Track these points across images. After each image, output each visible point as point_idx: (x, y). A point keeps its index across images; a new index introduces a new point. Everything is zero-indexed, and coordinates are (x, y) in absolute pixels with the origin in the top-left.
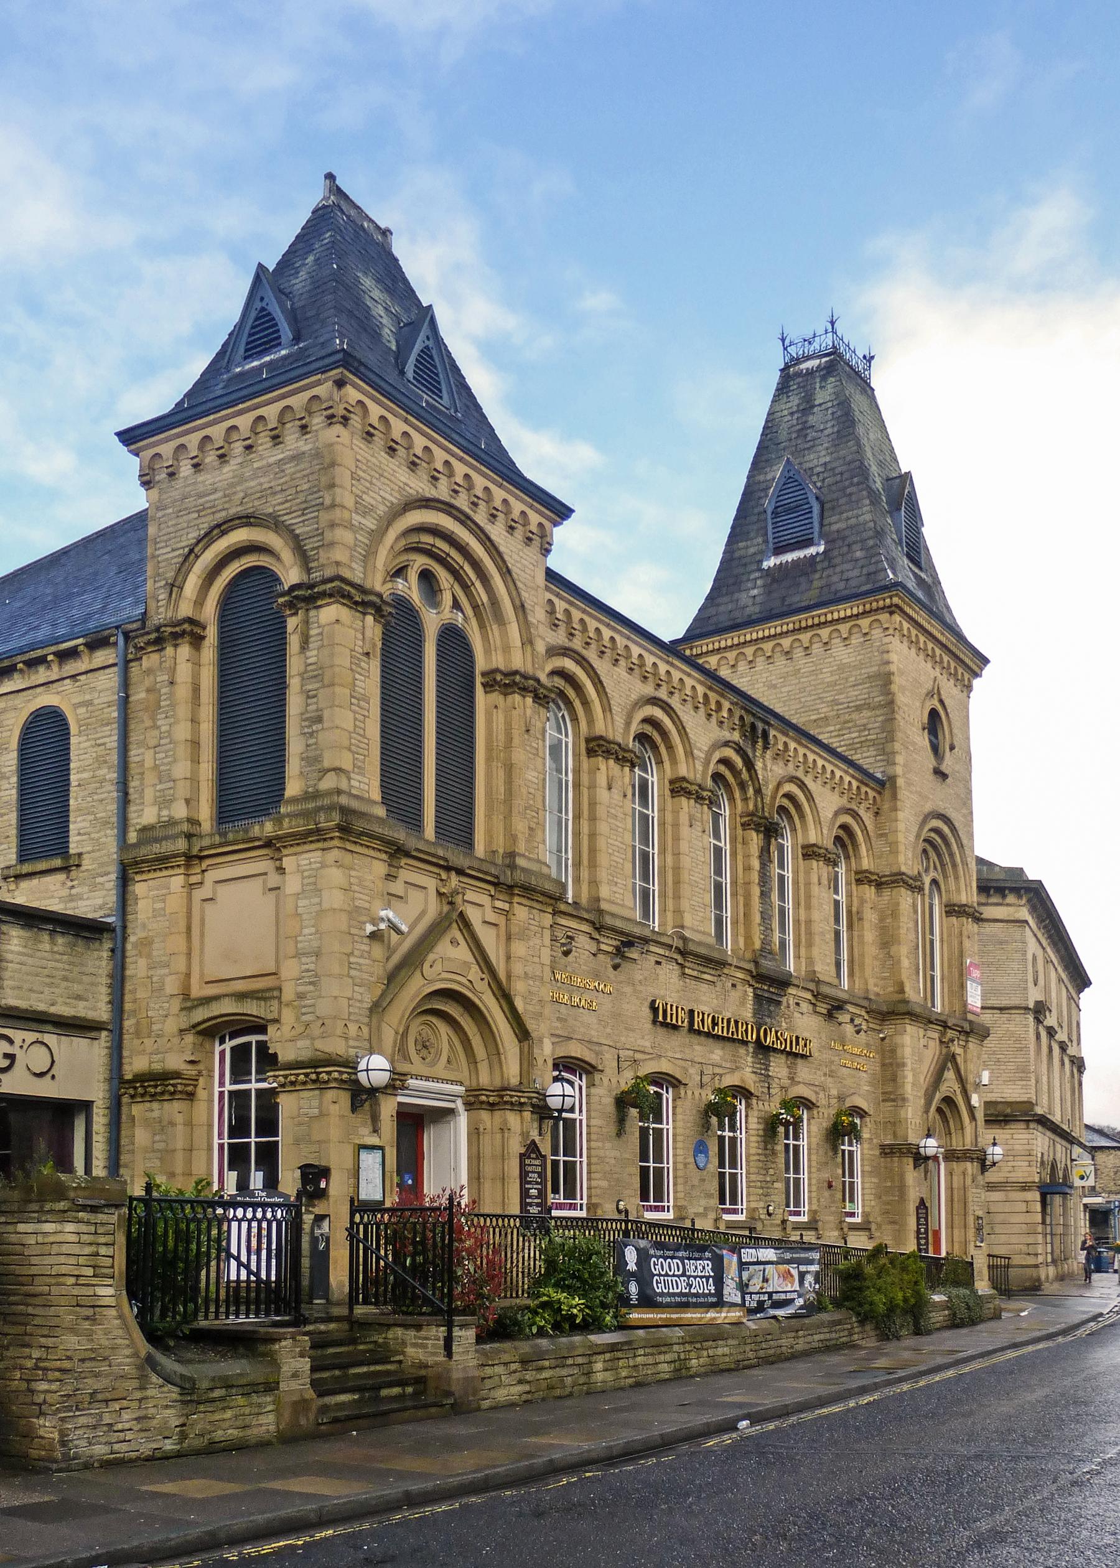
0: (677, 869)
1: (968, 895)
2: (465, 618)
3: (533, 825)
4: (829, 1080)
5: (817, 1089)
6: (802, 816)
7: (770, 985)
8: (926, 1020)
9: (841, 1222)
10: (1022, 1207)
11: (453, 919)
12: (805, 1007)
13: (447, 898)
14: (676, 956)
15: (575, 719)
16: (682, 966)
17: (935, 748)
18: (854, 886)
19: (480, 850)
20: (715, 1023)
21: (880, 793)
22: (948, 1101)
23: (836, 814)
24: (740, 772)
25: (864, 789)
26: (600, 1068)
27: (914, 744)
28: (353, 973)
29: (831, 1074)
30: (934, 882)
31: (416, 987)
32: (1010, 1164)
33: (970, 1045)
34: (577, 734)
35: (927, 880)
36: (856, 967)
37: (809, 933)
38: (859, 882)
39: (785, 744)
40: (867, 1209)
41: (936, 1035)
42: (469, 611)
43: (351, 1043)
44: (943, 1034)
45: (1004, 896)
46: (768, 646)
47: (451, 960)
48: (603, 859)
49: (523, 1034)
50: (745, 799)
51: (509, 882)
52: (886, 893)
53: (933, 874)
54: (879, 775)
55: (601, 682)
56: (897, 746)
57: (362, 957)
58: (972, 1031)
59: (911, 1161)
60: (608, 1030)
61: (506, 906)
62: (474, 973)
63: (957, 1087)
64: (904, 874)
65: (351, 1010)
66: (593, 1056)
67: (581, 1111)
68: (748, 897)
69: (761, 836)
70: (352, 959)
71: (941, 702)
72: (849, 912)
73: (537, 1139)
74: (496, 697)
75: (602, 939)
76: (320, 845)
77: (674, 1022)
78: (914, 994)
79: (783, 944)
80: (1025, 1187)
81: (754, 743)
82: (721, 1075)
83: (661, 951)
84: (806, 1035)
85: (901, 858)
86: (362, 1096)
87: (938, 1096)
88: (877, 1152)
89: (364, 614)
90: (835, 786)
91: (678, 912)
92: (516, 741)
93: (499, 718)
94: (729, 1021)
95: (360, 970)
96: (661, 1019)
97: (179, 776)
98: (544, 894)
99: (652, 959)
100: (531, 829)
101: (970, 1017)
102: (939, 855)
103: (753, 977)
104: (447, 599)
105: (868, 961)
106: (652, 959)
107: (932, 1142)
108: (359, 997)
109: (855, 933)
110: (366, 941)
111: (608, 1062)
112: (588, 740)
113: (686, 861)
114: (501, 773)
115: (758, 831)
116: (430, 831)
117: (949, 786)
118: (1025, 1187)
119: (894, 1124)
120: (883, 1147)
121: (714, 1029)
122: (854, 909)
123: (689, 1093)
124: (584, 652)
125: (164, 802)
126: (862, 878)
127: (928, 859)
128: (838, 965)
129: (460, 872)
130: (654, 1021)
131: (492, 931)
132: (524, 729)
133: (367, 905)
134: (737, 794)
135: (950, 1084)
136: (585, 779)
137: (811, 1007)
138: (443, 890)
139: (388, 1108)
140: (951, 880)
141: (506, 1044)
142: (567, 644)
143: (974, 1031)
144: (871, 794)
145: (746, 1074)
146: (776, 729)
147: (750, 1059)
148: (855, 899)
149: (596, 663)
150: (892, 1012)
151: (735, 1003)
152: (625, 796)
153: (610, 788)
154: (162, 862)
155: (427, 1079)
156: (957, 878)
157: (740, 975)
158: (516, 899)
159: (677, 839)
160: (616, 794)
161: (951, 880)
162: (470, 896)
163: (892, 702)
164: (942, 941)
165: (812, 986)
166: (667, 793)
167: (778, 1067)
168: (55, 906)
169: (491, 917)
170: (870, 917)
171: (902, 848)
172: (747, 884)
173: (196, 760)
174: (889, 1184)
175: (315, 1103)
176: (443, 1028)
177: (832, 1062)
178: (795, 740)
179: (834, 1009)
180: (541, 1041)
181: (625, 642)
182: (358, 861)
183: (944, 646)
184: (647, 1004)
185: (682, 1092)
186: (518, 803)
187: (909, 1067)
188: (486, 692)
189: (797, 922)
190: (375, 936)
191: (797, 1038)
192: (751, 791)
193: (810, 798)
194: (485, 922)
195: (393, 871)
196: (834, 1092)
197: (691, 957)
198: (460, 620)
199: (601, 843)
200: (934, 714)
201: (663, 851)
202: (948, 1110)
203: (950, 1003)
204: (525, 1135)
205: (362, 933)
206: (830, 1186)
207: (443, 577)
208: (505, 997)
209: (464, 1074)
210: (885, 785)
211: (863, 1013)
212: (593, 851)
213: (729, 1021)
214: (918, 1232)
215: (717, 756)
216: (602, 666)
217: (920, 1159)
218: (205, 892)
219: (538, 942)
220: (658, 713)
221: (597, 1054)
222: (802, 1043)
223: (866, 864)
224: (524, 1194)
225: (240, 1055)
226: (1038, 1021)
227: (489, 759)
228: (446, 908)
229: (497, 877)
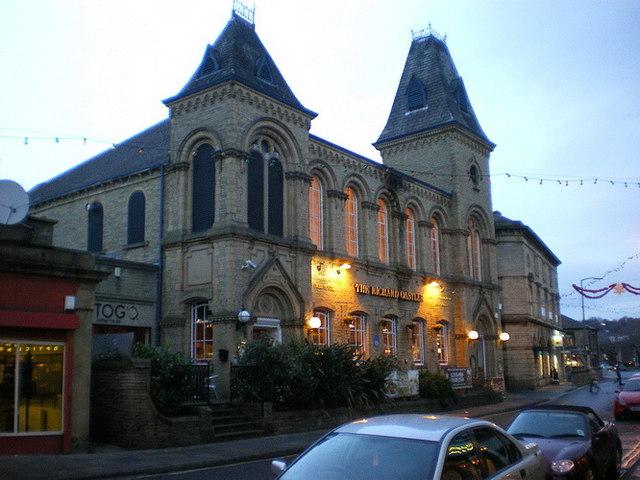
1: (491, 235)
6: (418, 211)
10: (525, 356)
11: (274, 261)
13: (272, 254)
15: (323, 184)
17: (475, 181)
19: (285, 235)
20: (381, 291)
22: (483, 316)
23: (432, 208)
30: (476, 230)
31: (260, 287)
35: (473, 230)
42: (280, 151)
47: (273, 277)
48: (334, 234)
56: (458, 181)
62: (282, 280)
80: (527, 348)
86: (240, 325)
90: (429, 197)
97: (179, 215)
116: (266, 230)
118: (527, 348)
125: (175, 224)
128: (435, 266)
131: (289, 265)
135: (484, 309)
139: (250, 329)
143: (493, 288)
149: (330, 164)
154: (174, 245)
162: (280, 252)
168: (140, 260)
170: (448, 247)
173: (186, 209)
176: (272, 300)
183: (476, 142)
190: (244, 270)
193: (420, 204)
200: (473, 168)
207: (271, 142)
208: (294, 288)
210: (452, 197)
212: (330, 232)
215: (381, 191)
218: (188, 255)
220: (356, 179)
223: (446, 226)
225: (200, 311)
226: (530, 281)
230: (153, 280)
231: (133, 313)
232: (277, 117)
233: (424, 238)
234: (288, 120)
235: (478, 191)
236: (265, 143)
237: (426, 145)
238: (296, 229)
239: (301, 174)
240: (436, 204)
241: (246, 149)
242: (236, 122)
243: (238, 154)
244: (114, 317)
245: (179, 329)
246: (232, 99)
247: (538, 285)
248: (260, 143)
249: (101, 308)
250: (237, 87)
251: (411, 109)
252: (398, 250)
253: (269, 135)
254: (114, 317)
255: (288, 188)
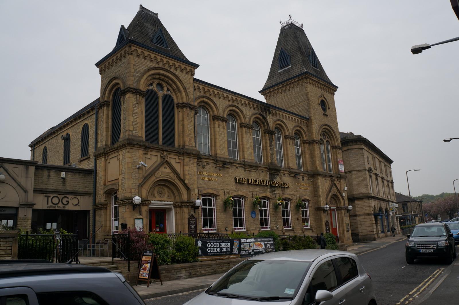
0: (243, 145)
2: (171, 92)
3: (190, 138)
4: (296, 193)
5: (292, 195)
7: (274, 170)
8: (325, 176)
9: (302, 228)
12: (286, 175)
14: (242, 166)
16: (245, 168)
18: (302, 145)
21: (307, 121)
22: (334, 195)
23: (294, 127)
24: (262, 120)
25: (302, 121)
26: (218, 195)
27: (316, 108)
28: (133, 177)
29: (297, 191)
30: (327, 141)
31: (153, 179)
32: (365, 209)
33: (341, 180)
34: (210, 116)
35: (325, 141)
36: (304, 164)
37: (288, 157)
38: (304, 143)
39: (276, 112)
40: (293, 225)
41: (330, 179)
43: (133, 194)
44: (332, 179)
45: (357, 143)
46: (280, 90)
47: (165, 172)
48: (218, 144)
49: (188, 188)
50: (264, 126)
51: (182, 152)
52: (311, 145)
53: (327, 139)
54: (307, 117)
55: (215, 103)
56: (311, 110)
57: (136, 173)
58: (341, 177)
59: (323, 212)
60: (221, 186)
61: (183, 158)
62: (172, 175)
63: (337, 191)
64: (315, 140)
65: (133, 186)
66: (216, 192)
67: (214, 206)
68: (267, 149)
69: (269, 134)
70: (133, 174)
71: (324, 98)
72: (302, 151)
73: (194, 214)
74: (180, 110)
75: (218, 164)
76: (125, 148)
77: (242, 182)
78: (320, 169)
79: (281, 160)
81: (266, 113)
82: (259, 194)
83: (238, 165)
84: (287, 182)
85: (314, 136)
87: (330, 194)
88: (314, 210)
89: (137, 95)
91: (243, 155)
92: (185, 118)
93: (181, 114)
94: (260, 181)
95: (136, 176)
96: (237, 182)
98: (193, 154)
99: (235, 167)
100: (189, 139)
101: (340, 173)
102: (328, 135)
103: (268, 169)
104: (165, 89)
105: (308, 162)
106: (235, 167)
107: (328, 206)
108: (135, 183)
109: (304, 156)
110: (137, 169)
111: (221, 193)
112: (213, 117)
113: (245, 143)
114: (181, 127)
115: (268, 134)
116: (160, 142)
117: (329, 117)
118: (369, 214)
119: (318, 202)
120: (315, 208)
121: (255, 183)
122: (303, 150)
123: (249, 199)
124: (210, 97)
126: (304, 142)
127: (325, 136)
129: (167, 151)
130: (236, 182)
131: (179, 164)
132: (187, 116)
133: (138, 161)
134: (262, 125)
135: (334, 190)
136: (212, 126)
137: (289, 175)
138: (162, 156)
140: (333, 140)
141: (183, 191)
142: (204, 95)
144: (305, 122)
145: (268, 194)
146: (272, 109)
147: (269, 189)
148: (303, 148)
150: (314, 175)
151: (263, 176)
152: (224, 129)
153: (219, 127)
155: (161, 201)
156: (334, 139)
157: (264, 169)
158: (185, 156)
159: (242, 137)
160: (221, 129)
161: (333, 140)
163: (308, 99)
164: (331, 155)
165: (288, 170)
166: (239, 126)
167: (279, 192)
169: (178, 161)
170: (307, 151)
171: (314, 134)
172: (266, 146)
174: (317, 218)
175: (125, 209)
177: (297, 188)
178: (278, 111)
179: (295, 175)
180: (194, 190)
181: (222, 93)
182: (134, 151)
184: (234, 178)
185: (246, 199)
186: (186, 133)
187: (320, 187)
188: (177, 108)
189: (284, 154)
190: (139, 168)
191: (284, 183)
192: (266, 124)
194: (176, 162)
195: (146, 152)
196: (298, 196)
197: (247, 166)
198: (169, 93)
199: (217, 140)
200: (322, 101)
201: (239, 141)
202: (335, 198)
203: (335, 171)
204: (189, 213)
205: (136, 168)
206: (298, 219)
209: (173, 199)
211: (306, 175)
212: (215, 142)
213: (260, 181)
214: (326, 229)
215: (254, 117)
216: (215, 100)
217: (325, 211)
218: (108, 161)
219: (193, 166)
221: (217, 191)
222: (285, 184)
223: (305, 138)
224: (190, 228)
227: (178, 124)
228: (163, 160)
229: (178, 151)
230: (90, 179)
231: (75, 202)
232: (167, 67)
233: (289, 146)
234: (176, 69)
235: (327, 115)
236: (159, 85)
237: (291, 89)
238: (184, 141)
239: (187, 104)
240: (297, 124)
241: (143, 87)
242: (133, 71)
243: (136, 92)
244: (60, 205)
245: (102, 211)
246: (130, 56)
247: (376, 175)
248: (155, 85)
249: (50, 199)
250: (133, 48)
251: (281, 68)
252: (269, 155)
253: (162, 79)
254: (60, 205)
255: (178, 114)
